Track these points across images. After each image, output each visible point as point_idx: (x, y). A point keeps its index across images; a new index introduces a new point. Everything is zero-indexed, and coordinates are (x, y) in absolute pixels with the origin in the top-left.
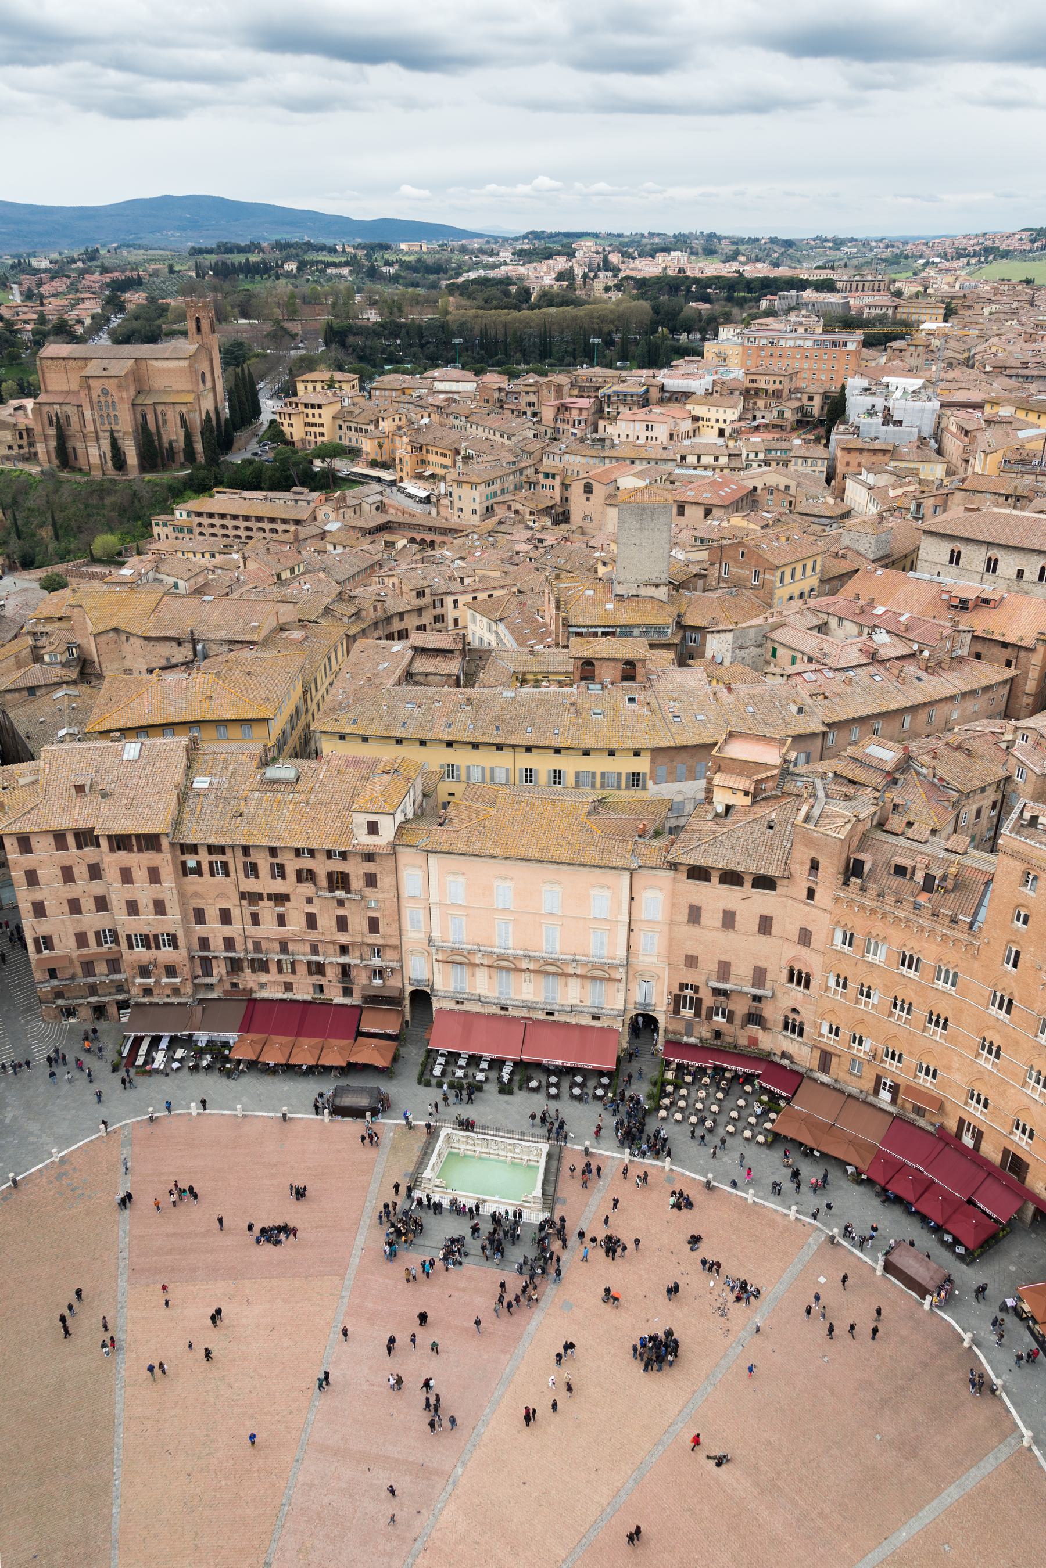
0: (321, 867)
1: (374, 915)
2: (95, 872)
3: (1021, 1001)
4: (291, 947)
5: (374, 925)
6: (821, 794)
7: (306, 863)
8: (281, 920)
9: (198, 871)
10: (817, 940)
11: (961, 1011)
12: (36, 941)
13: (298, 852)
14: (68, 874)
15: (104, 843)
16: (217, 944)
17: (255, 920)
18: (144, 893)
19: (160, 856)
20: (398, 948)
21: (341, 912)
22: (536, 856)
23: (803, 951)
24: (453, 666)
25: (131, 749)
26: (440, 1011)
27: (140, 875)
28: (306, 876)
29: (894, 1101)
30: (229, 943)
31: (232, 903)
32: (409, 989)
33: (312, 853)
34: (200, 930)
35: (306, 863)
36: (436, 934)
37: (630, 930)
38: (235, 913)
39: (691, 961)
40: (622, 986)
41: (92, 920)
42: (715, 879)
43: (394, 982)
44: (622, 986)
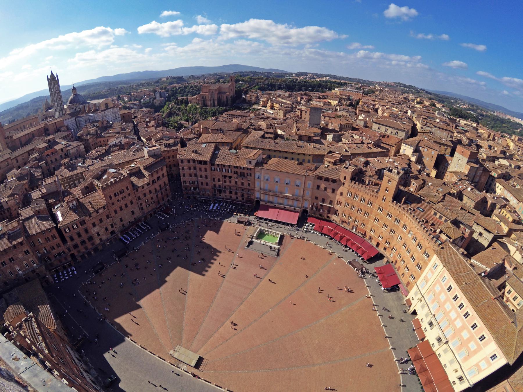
0: (239, 171)
1: (249, 182)
2: (195, 168)
3: (385, 209)
4: (232, 188)
5: (249, 185)
6: (348, 164)
7: (236, 170)
8: (230, 182)
9: (214, 170)
10: (345, 194)
11: (372, 211)
12: (183, 182)
13: (234, 167)
14: (190, 169)
15: (196, 162)
16: (217, 186)
17: (225, 182)
18: (203, 173)
19: (207, 166)
20: (253, 190)
21: (242, 181)
22: (285, 171)
23: (341, 197)
24: (272, 136)
25: (204, 145)
26: (262, 205)
27: (203, 169)
28: (236, 173)
29: (356, 231)
30: (220, 186)
31: (220, 177)
32: (256, 199)
33: (237, 167)
34: (214, 183)
35: (236, 170)
36: (262, 187)
37: (304, 190)
38: (221, 180)
39: (316, 198)
40: (301, 202)
41: (194, 178)
42: (323, 180)
43: (252, 197)
44: (301, 202)
